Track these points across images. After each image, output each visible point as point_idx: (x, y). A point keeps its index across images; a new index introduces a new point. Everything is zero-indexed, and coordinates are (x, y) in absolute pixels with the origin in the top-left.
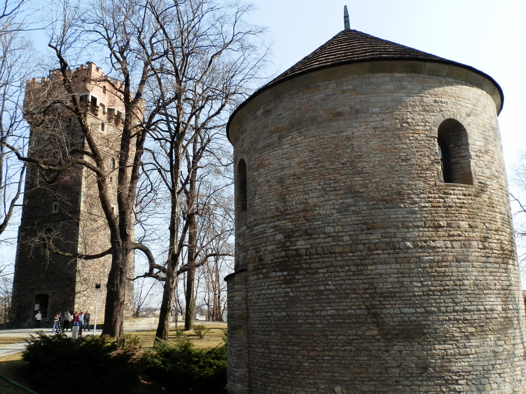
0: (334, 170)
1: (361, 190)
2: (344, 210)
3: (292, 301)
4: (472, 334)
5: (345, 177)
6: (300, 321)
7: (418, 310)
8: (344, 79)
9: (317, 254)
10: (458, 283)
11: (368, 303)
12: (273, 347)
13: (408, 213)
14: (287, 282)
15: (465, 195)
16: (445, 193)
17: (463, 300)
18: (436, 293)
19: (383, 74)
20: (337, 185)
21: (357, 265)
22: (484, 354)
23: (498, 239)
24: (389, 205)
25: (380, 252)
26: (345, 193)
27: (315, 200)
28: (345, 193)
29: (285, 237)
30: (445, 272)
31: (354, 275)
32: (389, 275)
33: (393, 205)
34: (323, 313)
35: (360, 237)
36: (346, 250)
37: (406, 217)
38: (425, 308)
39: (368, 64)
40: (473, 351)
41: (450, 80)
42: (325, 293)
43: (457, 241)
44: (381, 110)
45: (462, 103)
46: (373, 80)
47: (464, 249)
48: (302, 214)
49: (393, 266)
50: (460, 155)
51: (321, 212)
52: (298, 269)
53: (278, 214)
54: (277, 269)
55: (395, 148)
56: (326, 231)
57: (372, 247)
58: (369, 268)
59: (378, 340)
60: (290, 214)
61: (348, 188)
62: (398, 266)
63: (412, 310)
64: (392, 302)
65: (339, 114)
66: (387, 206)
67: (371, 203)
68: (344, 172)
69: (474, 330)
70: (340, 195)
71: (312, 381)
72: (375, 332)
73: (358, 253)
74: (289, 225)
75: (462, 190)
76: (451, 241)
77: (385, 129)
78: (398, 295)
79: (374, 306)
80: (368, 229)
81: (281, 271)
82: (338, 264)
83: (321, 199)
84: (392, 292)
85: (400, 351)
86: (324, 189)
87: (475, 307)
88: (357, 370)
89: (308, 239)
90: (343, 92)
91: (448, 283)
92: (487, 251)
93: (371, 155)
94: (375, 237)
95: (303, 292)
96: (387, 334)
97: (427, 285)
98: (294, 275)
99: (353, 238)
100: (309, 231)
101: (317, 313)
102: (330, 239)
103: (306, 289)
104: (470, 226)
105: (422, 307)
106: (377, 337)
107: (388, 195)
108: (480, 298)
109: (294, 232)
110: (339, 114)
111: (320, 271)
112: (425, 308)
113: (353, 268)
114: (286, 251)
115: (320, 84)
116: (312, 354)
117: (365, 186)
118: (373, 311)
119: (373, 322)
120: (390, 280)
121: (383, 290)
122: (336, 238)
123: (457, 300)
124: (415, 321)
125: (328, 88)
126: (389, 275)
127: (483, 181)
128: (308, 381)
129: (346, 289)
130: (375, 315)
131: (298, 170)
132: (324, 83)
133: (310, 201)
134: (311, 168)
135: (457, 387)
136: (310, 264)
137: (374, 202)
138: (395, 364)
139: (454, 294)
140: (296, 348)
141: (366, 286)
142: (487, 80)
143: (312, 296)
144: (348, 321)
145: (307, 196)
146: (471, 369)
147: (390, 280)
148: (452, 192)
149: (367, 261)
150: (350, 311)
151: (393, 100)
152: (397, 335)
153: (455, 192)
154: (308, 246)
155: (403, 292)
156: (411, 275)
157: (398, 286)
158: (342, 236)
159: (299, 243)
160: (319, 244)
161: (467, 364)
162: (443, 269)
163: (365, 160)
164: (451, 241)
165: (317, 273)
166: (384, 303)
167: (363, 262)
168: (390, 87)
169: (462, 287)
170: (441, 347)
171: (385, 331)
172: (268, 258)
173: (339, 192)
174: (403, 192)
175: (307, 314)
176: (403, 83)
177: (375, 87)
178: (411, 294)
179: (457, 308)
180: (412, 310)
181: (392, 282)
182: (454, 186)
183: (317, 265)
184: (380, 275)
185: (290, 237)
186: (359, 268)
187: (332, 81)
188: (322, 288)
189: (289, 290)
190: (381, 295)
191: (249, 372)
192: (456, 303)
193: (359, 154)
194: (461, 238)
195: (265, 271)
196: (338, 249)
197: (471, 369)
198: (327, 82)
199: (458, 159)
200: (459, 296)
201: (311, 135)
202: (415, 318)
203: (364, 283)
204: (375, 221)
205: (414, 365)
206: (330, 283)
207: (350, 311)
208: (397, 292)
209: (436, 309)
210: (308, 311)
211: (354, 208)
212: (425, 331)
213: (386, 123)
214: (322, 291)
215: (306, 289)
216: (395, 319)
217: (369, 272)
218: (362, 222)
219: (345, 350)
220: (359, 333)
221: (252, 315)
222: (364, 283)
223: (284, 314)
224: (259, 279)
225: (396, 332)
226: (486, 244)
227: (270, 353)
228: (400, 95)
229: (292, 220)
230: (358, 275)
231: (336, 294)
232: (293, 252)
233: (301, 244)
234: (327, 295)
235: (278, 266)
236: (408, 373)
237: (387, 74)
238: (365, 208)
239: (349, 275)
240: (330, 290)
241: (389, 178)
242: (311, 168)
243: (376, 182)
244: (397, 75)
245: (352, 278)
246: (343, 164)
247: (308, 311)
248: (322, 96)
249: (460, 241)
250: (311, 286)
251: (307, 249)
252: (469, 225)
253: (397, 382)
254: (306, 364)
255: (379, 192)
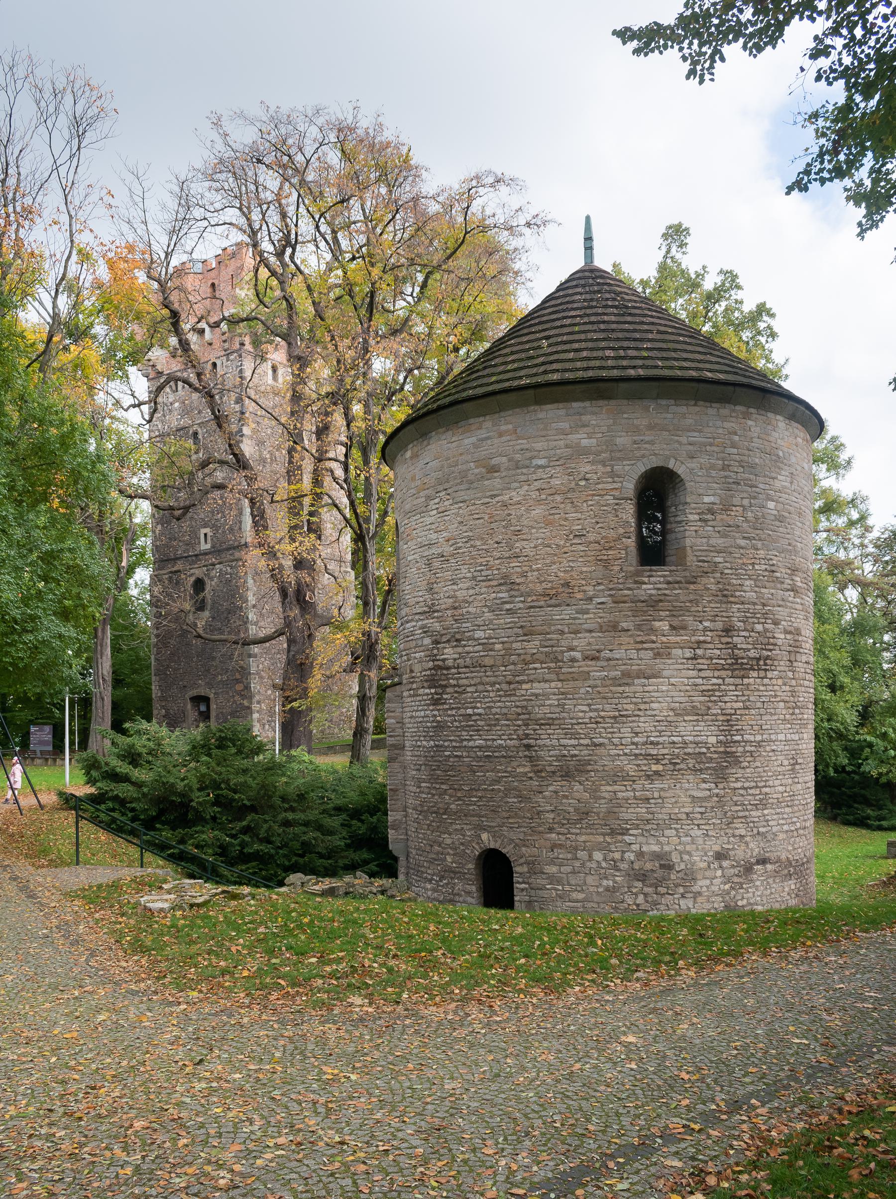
0: (487, 551)
1: (518, 581)
2: (496, 608)
3: (440, 727)
4: (657, 773)
5: (497, 562)
6: (447, 753)
7: (582, 741)
8: (502, 414)
9: (466, 667)
10: (642, 707)
11: (520, 732)
12: (423, 785)
13: (577, 613)
14: (436, 702)
15: (669, 583)
16: (636, 582)
17: (648, 729)
18: (607, 720)
19: (556, 405)
20: (489, 572)
21: (510, 683)
22: (674, 800)
23: (728, 643)
24: (553, 602)
25: (538, 665)
26: (500, 585)
27: (464, 593)
28: (500, 585)
29: (433, 643)
30: (624, 692)
31: (506, 696)
32: (546, 696)
33: (557, 602)
34: (471, 744)
35: (514, 645)
36: (498, 663)
37: (575, 619)
38: (591, 739)
39: (531, 392)
40: (656, 795)
41: (664, 402)
42: (474, 718)
43: (646, 649)
44: (550, 461)
45: (680, 439)
46: (541, 415)
47: (658, 661)
48: (449, 613)
49: (553, 685)
50: (678, 519)
51: (470, 609)
52: (446, 686)
53: (426, 609)
54: (426, 684)
55: (566, 519)
56: (476, 636)
57: (528, 658)
58: (524, 686)
59: (531, 778)
60: (438, 611)
61: (502, 578)
62: (560, 684)
63: (573, 742)
64: (549, 731)
65: (494, 469)
66: (549, 602)
67: (529, 599)
68: (499, 555)
69: (660, 768)
70: (492, 586)
71: (458, 827)
72: (527, 769)
73: (511, 667)
74: (437, 626)
75: (664, 576)
76: (638, 650)
77: (553, 491)
78: (556, 722)
79: (527, 736)
80: (525, 635)
81: (430, 688)
82: (487, 680)
83: (471, 592)
84: (549, 719)
85: (556, 792)
86: (474, 578)
87: (666, 738)
88: (505, 815)
89: (456, 646)
90: (500, 435)
91: (625, 706)
92: (699, 661)
93: (534, 531)
94: (533, 645)
95: (449, 716)
96: (541, 771)
97: (596, 710)
98: (441, 694)
99: (506, 646)
100: (458, 636)
101: (465, 743)
102: (480, 648)
103: (454, 712)
104: (673, 628)
105: (587, 736)
106: (530, 775)
107: (552, 588)
108: (676, 727)
109: (442, 635)
110: (494, 469)
111: (469, 689)
112: (591, 739)
113: (505, 687)
114: (433, 661)
115: (472, 421)
116: (459, 795)
117: (524, 575)
118: (524, 742)
119: (525, 756)
120: (548, 702)
121: (539, 716)
122: (487, 646)
123: (638, 730)
124: (576, 756)
125: (481, 429)
126: (546, 696)
127: (709, 559)
128: (454, 827)
129: (497, 714)
130: (528, 747)
131: (448, 549)
132: (477, 420)
133: (458, 594)
134: (460, 548)
135: (626, 838)
136: (457, 679)
137: (534, 598)
138: (548, 808)
139: (634, 721)
140: (444, 787)
141: (519, 710)
142: (738, 389)
143: (460, 722)
144: (496, 754)
145: (455, 587)
146: (650, 816)
147: (548, 702)
148: (646, 580)
149: (521, 678)
150: (500, 742)
151: (567, 446)
152: (554, 772)
153: (652, 579)
154: (457, 656)
155: (564, 718)
156: (576, 696)
157: (558, 710)
158: (494, 644)
159: (446, 651)
160: (468, 653)
161: (644, 810)
162: (620, 689)
163: (524, 537)
164: (638, 650)
165: (464, 692)
166: (539, 732)
167: (517, 679)
168: (565, 425)
169: (648, 713)
170: (609, 788)
171: (539, 768)
172: (417, 668)
173: (492, 583)
174: (573, 583)
175: (454, 744)
176: (584, 418)
177: (542, 426)
178: (574, 721)
179: (636, 740)
180: (573, 742)
181: (550, 705)
182: (651, 570)
183: (465, 682)
184: (537, 695)
185: (437, 642)
186: (512, 686)
187: (488, 417)
188: (470, 711)
189: (436, 713)
190: (537, 722)
191: (406, 816)
192: (637, 734)
193: (518, 528)
194: (654, 646)
195: (414, 686)
196: (488, 661)
197: (650, 816)
198: (481, 419)
199: (674, 525)
200: (641, 724)
201: (460, 499)
202: (576, 752)
203: (517, 707)
204: (534, 624)
205: (572, 810)
206: (479, 705)
207: (500, 742)
208: (557, 719)
209: (606, 741)
210: (455, 741)
211: (508, 606)
212: (589, 768)
213: (556, 482)
214: (470, 715)
215: (454, 712)
216: (551, 753)
217: (523, 692)
218: (518, 625)
219: (493, 790)
220: (509, 769)
221: (407, 744)
222: (517, 707)
223: (432, 743)
224: (410, 696)
225: (552, 769)
226: (699, 652)
227: (420, 792)
228: (579, 436)
229: (440, 619)
230: (510, 695)
231: (485, 720)
232: (440, 663)
233: (449, 653)
234: (475, 721)
235: (426, 681)
236: (564, 818)
237: (561, 405)
238: (521, 605)
239: (500, 696)
240: (480, 715)
241: (554, 563)
242: (460, 548)
243: (538, 570)
244: (575, 405)
245: (503, 699)
246: (497, 543)
247: (455, 741)
248: (474, 439)
249: (652, 649)
250: (459, 708)
251: (455, 659)
252: (671, 626)
253: (551, 830)
254: (453, 806)
255: (541, 583)
